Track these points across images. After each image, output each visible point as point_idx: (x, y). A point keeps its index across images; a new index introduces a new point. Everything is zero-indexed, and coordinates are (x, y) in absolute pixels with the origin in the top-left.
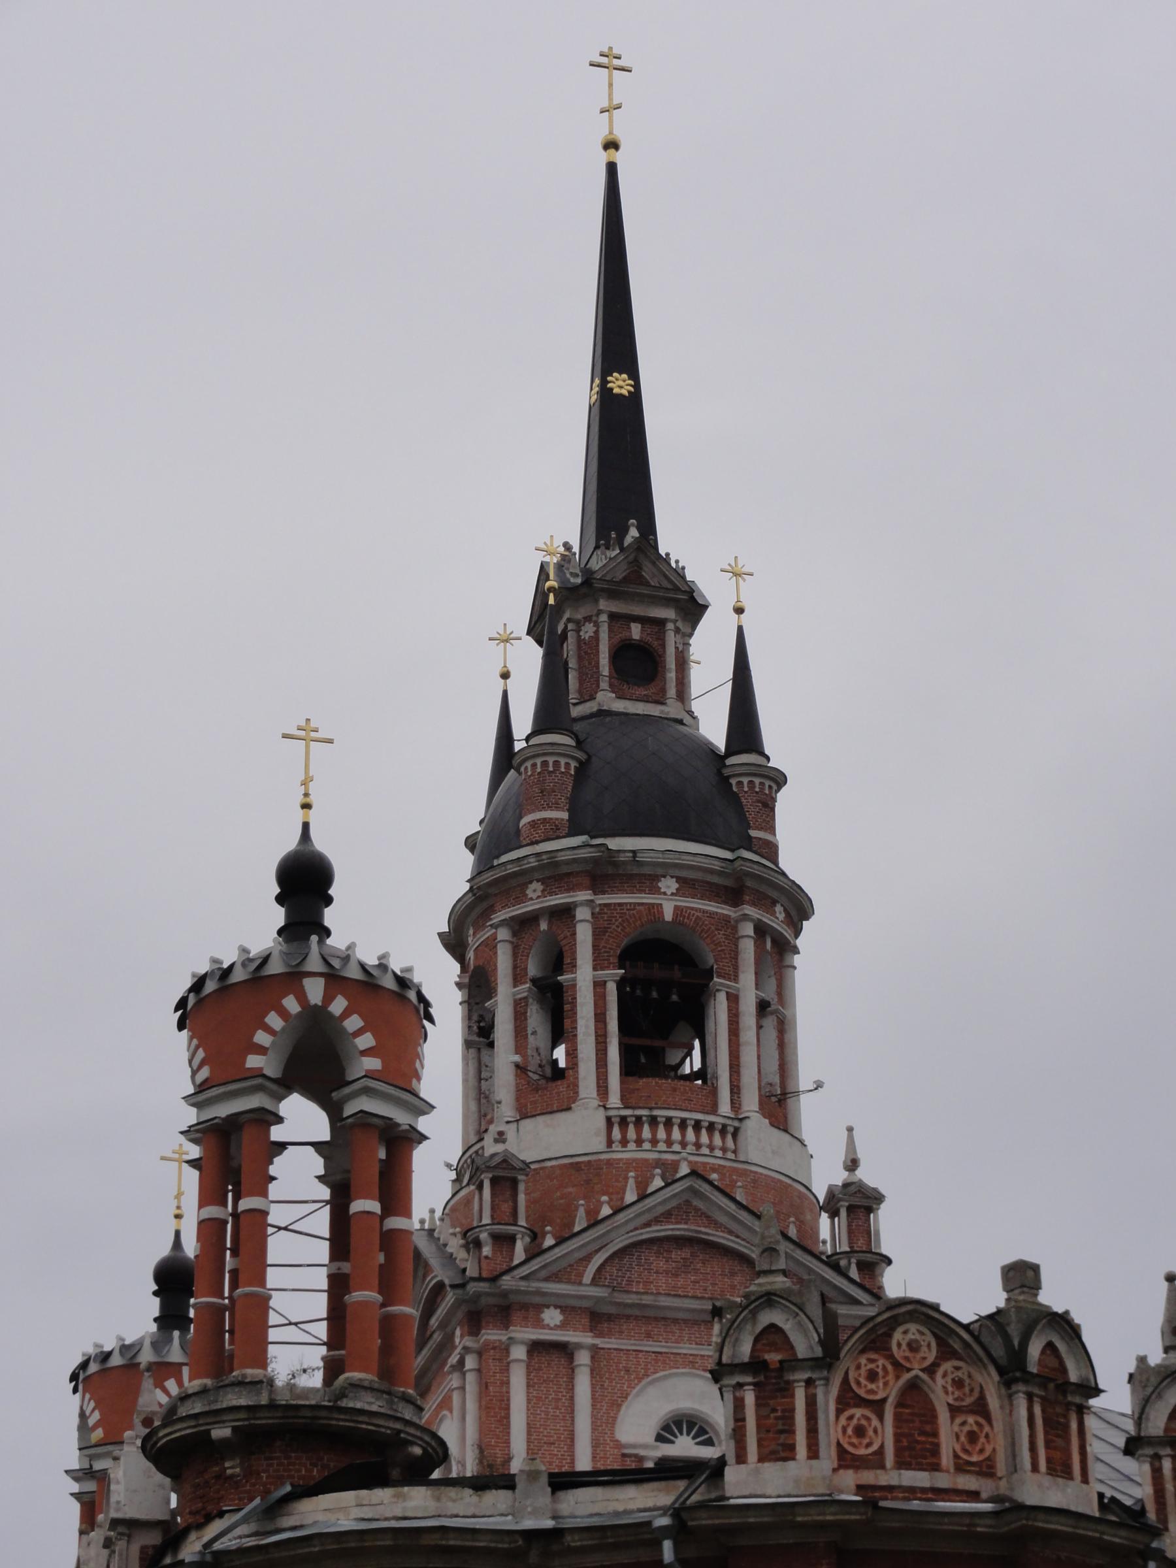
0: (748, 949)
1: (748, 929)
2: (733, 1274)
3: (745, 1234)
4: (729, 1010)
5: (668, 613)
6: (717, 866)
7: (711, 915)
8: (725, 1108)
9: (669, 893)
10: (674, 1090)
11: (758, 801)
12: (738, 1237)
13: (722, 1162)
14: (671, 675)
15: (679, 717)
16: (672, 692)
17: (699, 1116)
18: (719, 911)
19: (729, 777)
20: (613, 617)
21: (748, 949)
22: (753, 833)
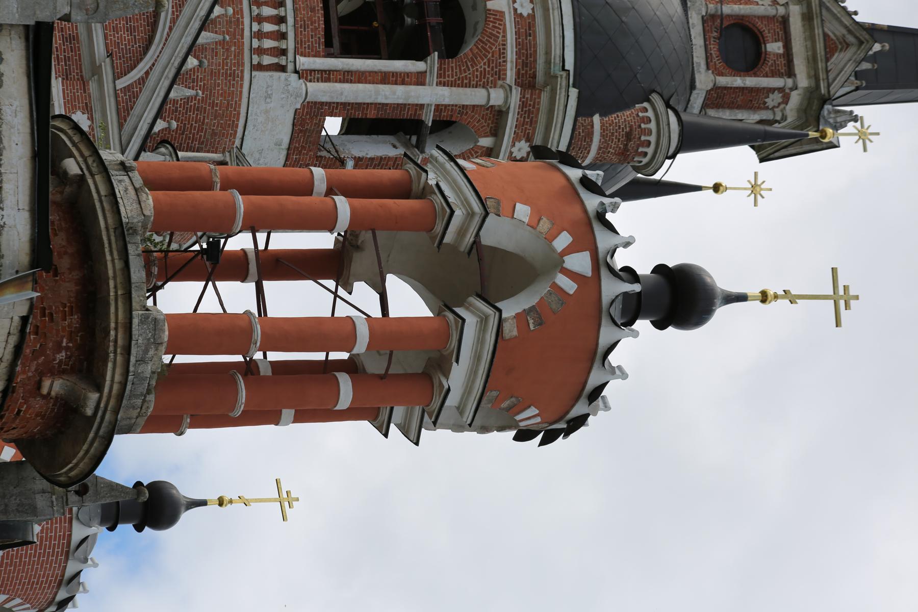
0: (474, 96)
1: (497, 97)
2: (131, 30)
3: (175, 34)
4: (408, 74)
5: (803, 81)
6: (556, 51)
7: (502, 54)
8: (305, 62)
9: (516, 5)
10: (313, 10)
11: (631, 127)
12: (171, 29)
13: (247, 33)
14: (738, 82)
15: (698, 84)
16: (723, 81)
17: (290, 20)
18: (509, 65)
19: (649, 100)
20: (785, 21)
21: (474, 96)
22: (596, 119)
